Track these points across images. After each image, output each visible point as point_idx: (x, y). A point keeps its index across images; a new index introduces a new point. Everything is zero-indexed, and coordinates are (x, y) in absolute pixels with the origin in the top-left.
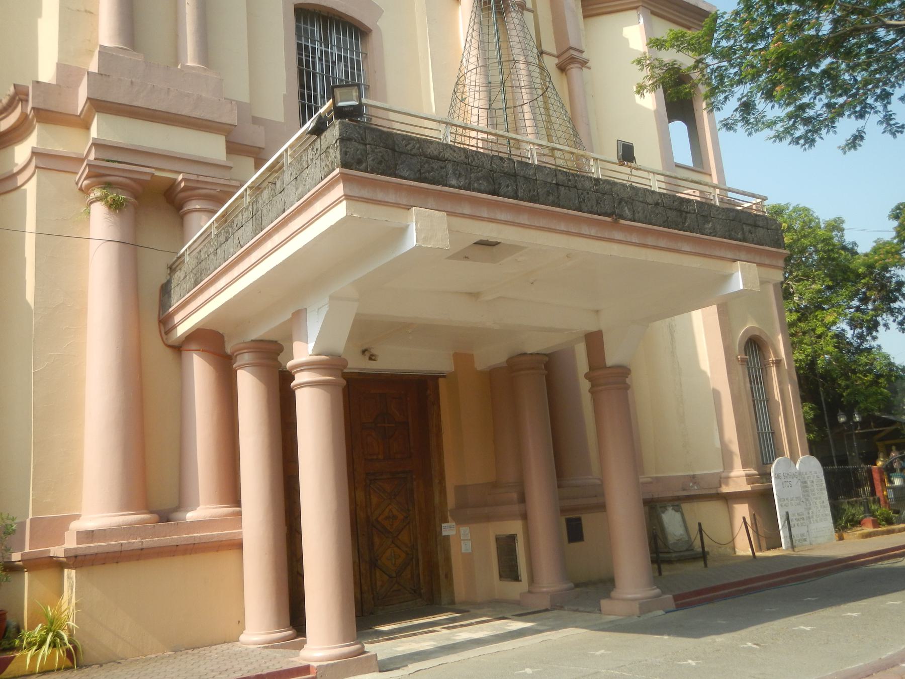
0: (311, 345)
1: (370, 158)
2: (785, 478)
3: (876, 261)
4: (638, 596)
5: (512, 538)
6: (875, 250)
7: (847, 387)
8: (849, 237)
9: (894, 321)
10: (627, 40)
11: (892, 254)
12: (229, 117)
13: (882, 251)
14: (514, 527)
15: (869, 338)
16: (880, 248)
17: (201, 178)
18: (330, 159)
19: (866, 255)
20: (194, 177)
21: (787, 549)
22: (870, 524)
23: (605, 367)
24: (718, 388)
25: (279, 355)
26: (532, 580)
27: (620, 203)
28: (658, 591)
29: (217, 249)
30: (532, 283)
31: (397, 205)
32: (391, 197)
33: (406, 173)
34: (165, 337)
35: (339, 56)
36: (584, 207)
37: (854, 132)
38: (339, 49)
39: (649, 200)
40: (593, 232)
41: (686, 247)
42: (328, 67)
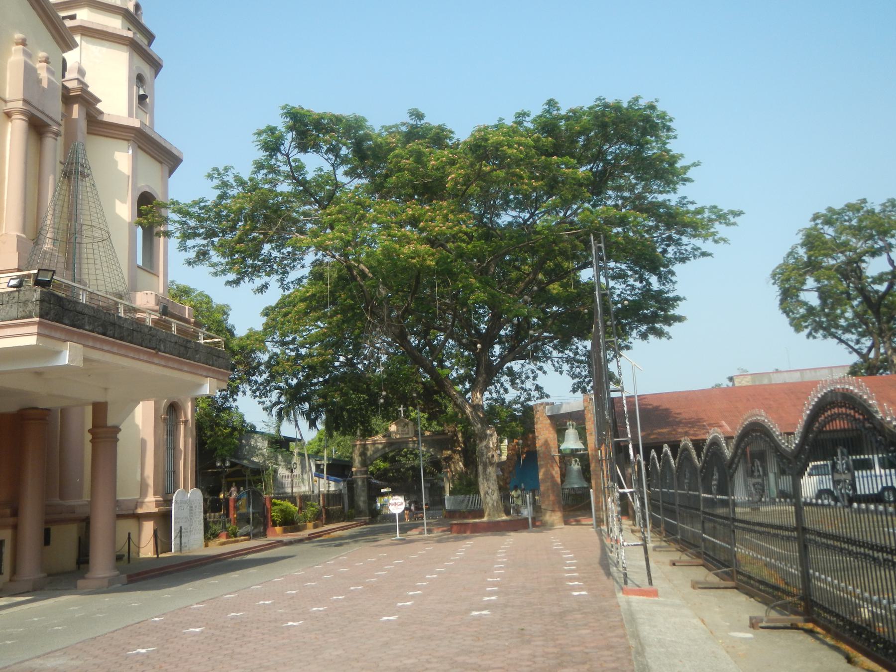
1: (52, 312)
2: (179, 503)
3: (248, 345)
4: (107, 575)
6: (248, 337)
7: (211, 436)
8: (231, 321)
9: (250, 389)
13: (253, 338)
15: (231, 400)
18: (28, 309)
19: (241, 339)
21: (175, 552)
22: (225, 537)
23: (105, 426)
24: (146, 438)
26: (14, 571)
28: (117, 573)
31: (59, 339)
32: (58, 335)
33: (67, 321)
36: (144, 344)
37: (264, 283)
40: (145, 358)
41: (186, 369)
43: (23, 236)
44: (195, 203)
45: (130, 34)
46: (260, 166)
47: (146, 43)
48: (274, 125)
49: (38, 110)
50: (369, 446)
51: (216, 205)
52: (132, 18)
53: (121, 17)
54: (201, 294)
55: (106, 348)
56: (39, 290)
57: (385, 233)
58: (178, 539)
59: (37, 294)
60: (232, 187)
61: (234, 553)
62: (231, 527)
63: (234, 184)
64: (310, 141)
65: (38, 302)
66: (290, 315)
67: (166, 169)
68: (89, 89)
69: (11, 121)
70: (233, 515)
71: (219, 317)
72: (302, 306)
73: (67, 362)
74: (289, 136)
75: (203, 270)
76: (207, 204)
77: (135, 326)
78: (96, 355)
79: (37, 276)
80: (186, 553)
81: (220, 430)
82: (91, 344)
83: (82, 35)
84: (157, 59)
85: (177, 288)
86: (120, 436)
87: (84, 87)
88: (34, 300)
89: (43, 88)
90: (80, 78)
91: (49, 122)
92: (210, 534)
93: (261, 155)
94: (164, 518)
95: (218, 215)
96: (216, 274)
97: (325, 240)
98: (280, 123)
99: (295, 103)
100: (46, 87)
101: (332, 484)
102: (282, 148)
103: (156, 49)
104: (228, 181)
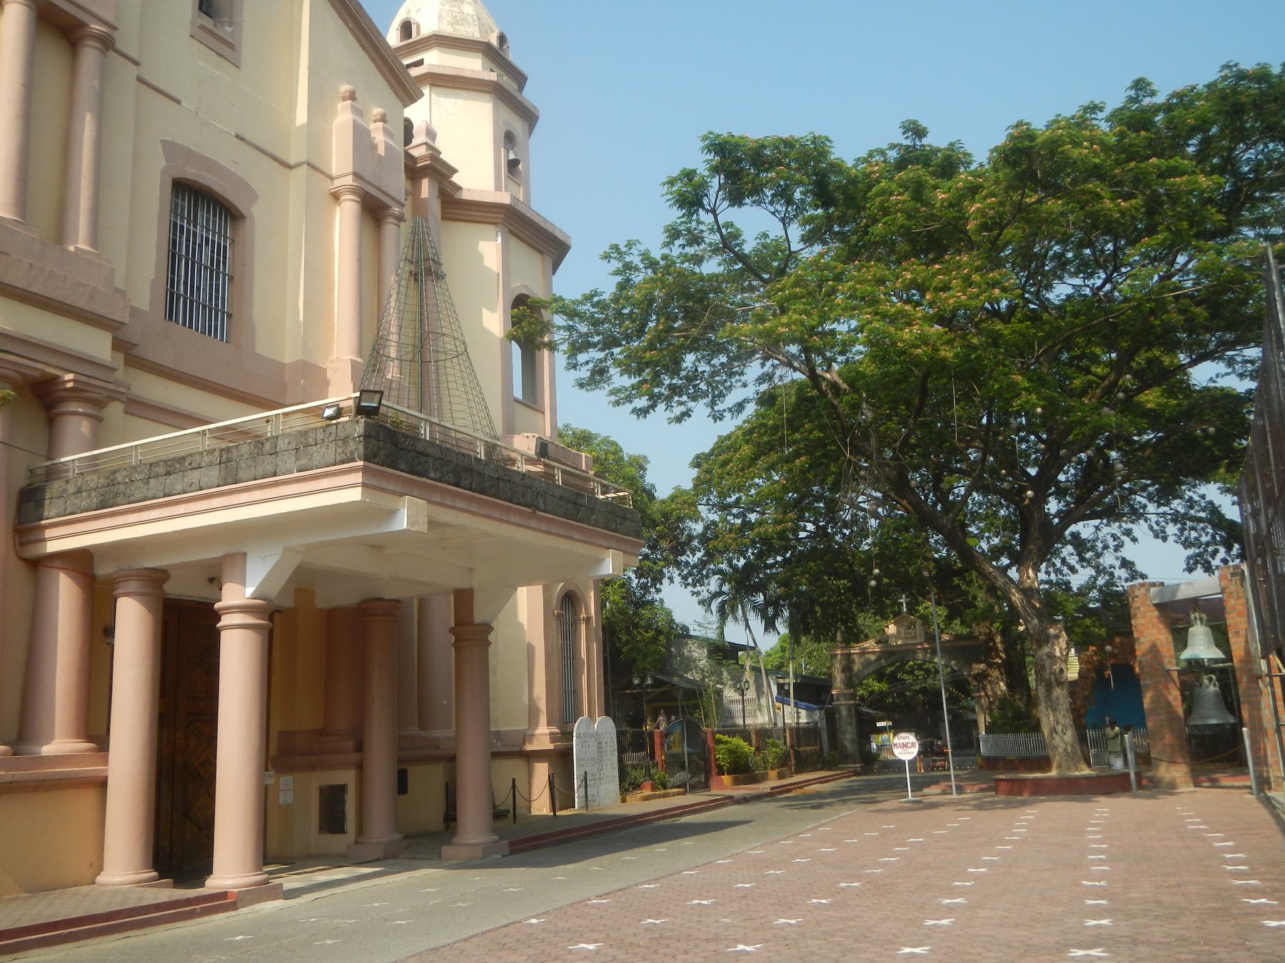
0: (249, 591)
1: (382, 452)
2: (583, 737)
3: (673, 510)
5: (342, 789)
6: (673, 498)
7: (628, 642)
8: (650, 478)
9: (679, 575)
10: (481, 257)
11: (689, 504)
12: (121, 315)
13: (679, 500)
14: (347, 777)
15: (652, 590)
16: (677, 497)
17: (92, 381)
18: (349, 449)
19: (663, 502)
20: (84, 379)
21: (579, 809)
22: (649, 788)
23: (472, 624)
24: (534, 642)
25: (164, 583)
26: (361, 830)
27: (537, 496)
28: (496, 837)
29: (149, 478)
30: (443, 548)
31: (393, 493)
32: (391, 487)
33: (403, 467)
34: (18, 547)
35: (207, 239)
36: (515, 500)
38: (207, 232)
39: (556, 494)
40: (517, 520)
41: (577, 536)
42: (194, 250)
43: (360, 360)
44: (588, 298)
45: (493, 77)
46: (673, 233)
47: (516, 88)
48: (692, 167)
49: (374, 186)
50: (856, 657)
51: (616, 300)
52: (495, 54)
53: (480, 55)
54: (606, 441)
55: (460, 504)
56: (363, 420)
57: (870, 310)
58: (583, 790)
59: (360, 429)
60: (637, 269)
61: (663, 814)
62: (658, 773)
63: (641, 266)
64: (747, 183)
65: (362, 439)
66: (731, 465)
67: (549, 262)
68: (442, 156)
69: (339, 205)
70: (660, 757)
71: (631, 471)
72: (746, 450)
73: (405, 526)
74: (715, 183)
75: (600, 395)
76: (602, 298)
77: (501, 473)
78: (446, 516)
79: (360, 402)
80: (594, 810)
81: (640, 633)
82: (438, 499)
83: (432, 85)
84: (532, 109)
85: (574, 434)
86: (491, 637)
87: (434, 155)
88: (356, 435)
89: (380, 156)
90: (430, 142)
91: (389, 202)
92: (628, 784)
93: (674, 215)
94: (562, 758)
95: (619, 314)
96: (617, 403)
97: (777, 327)
98: (700, 162)
99: (723, 129)
100: (383, 154)
101: (803, 713)
102: (705, 201)
103: (530, 95)
104: (631, 262)
